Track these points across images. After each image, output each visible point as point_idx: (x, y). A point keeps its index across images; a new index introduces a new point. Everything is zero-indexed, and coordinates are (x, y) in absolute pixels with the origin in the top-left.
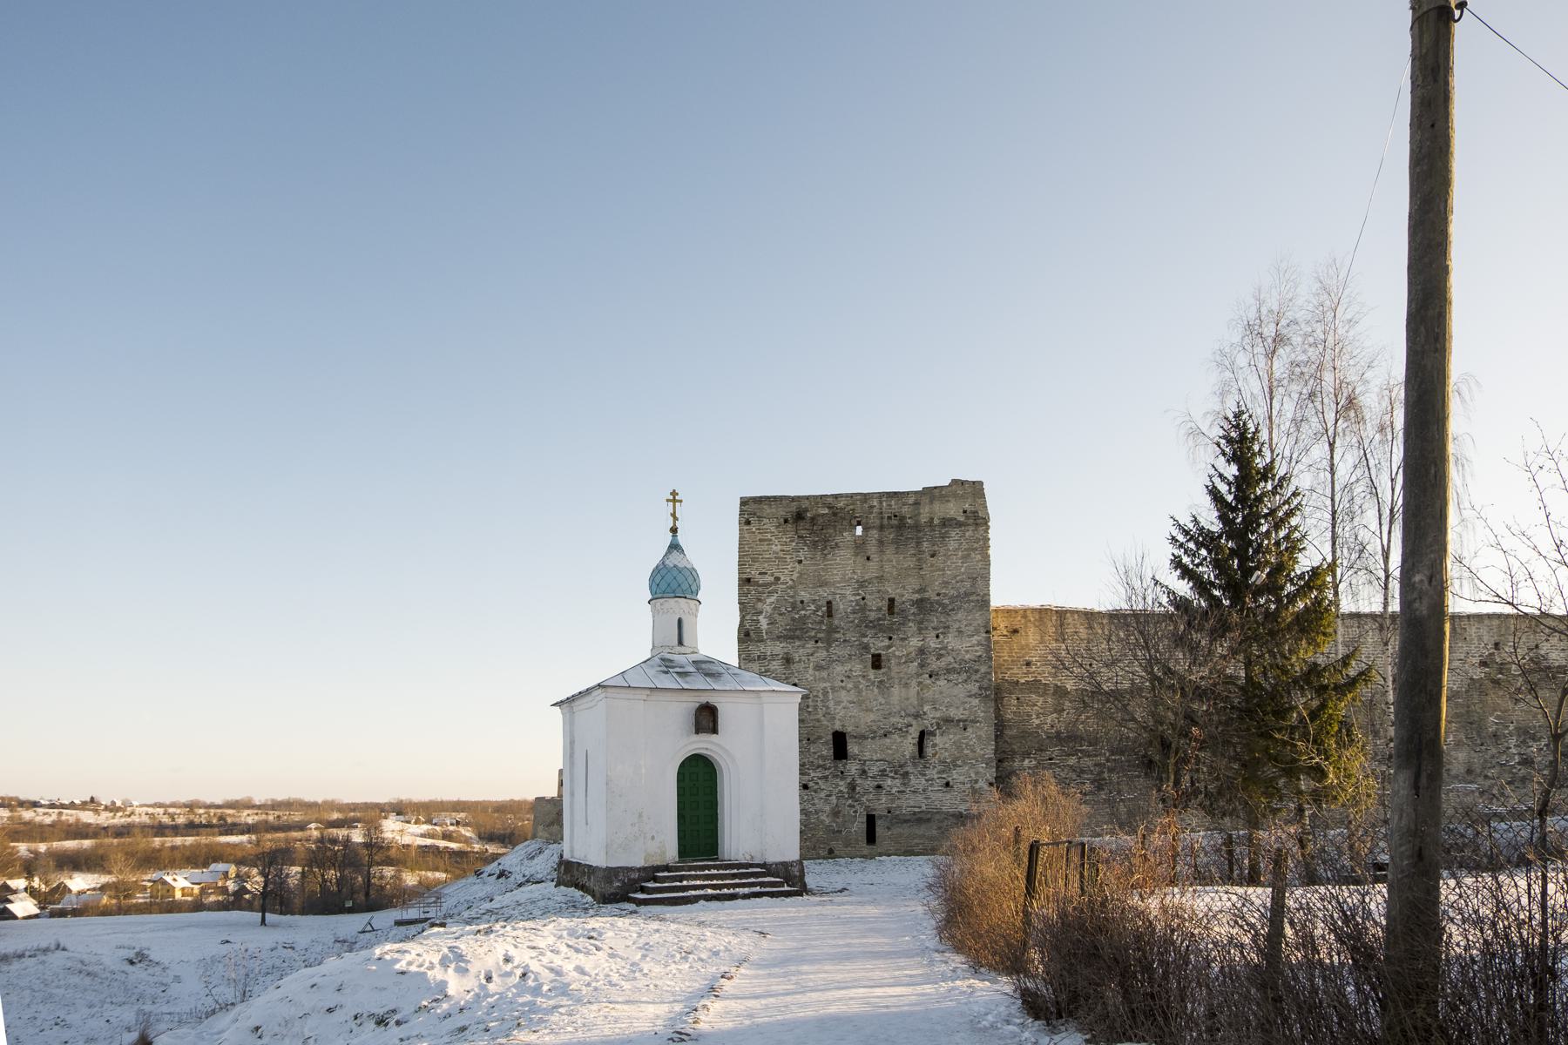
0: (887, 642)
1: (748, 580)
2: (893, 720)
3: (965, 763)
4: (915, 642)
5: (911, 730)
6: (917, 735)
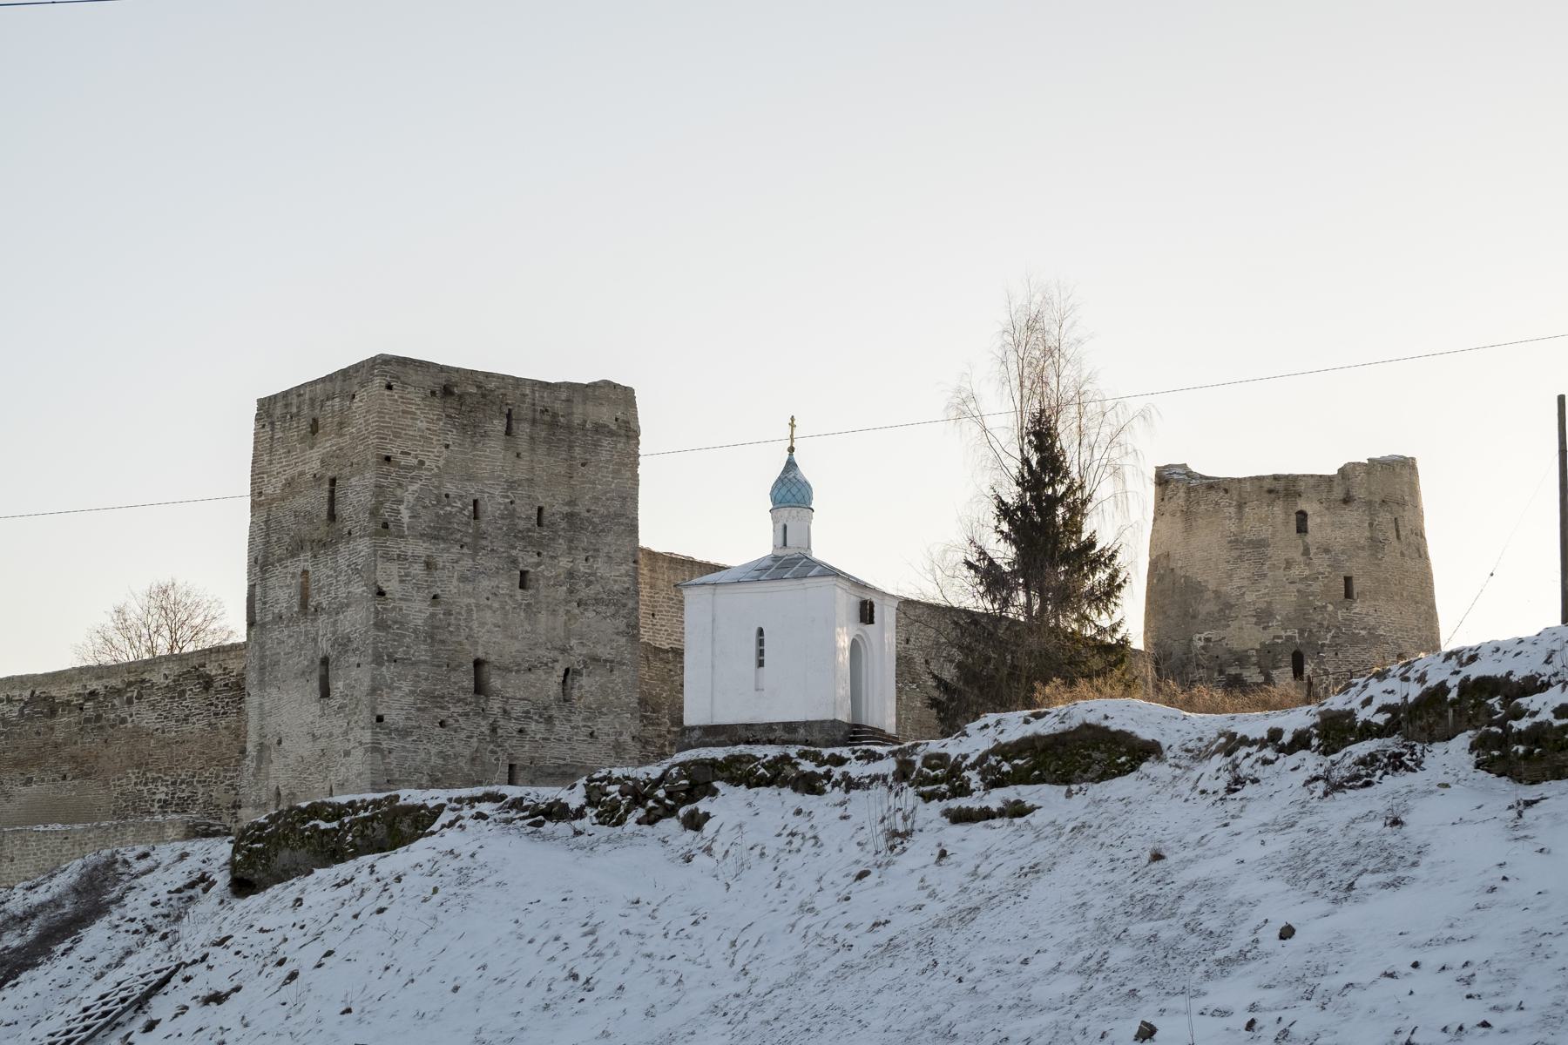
0: (536, 559)
1: (388, 459)
2: (539, 652)
3: (611, 712)
4: (564, 562)
5: (558, 666)
6: (562, 673)
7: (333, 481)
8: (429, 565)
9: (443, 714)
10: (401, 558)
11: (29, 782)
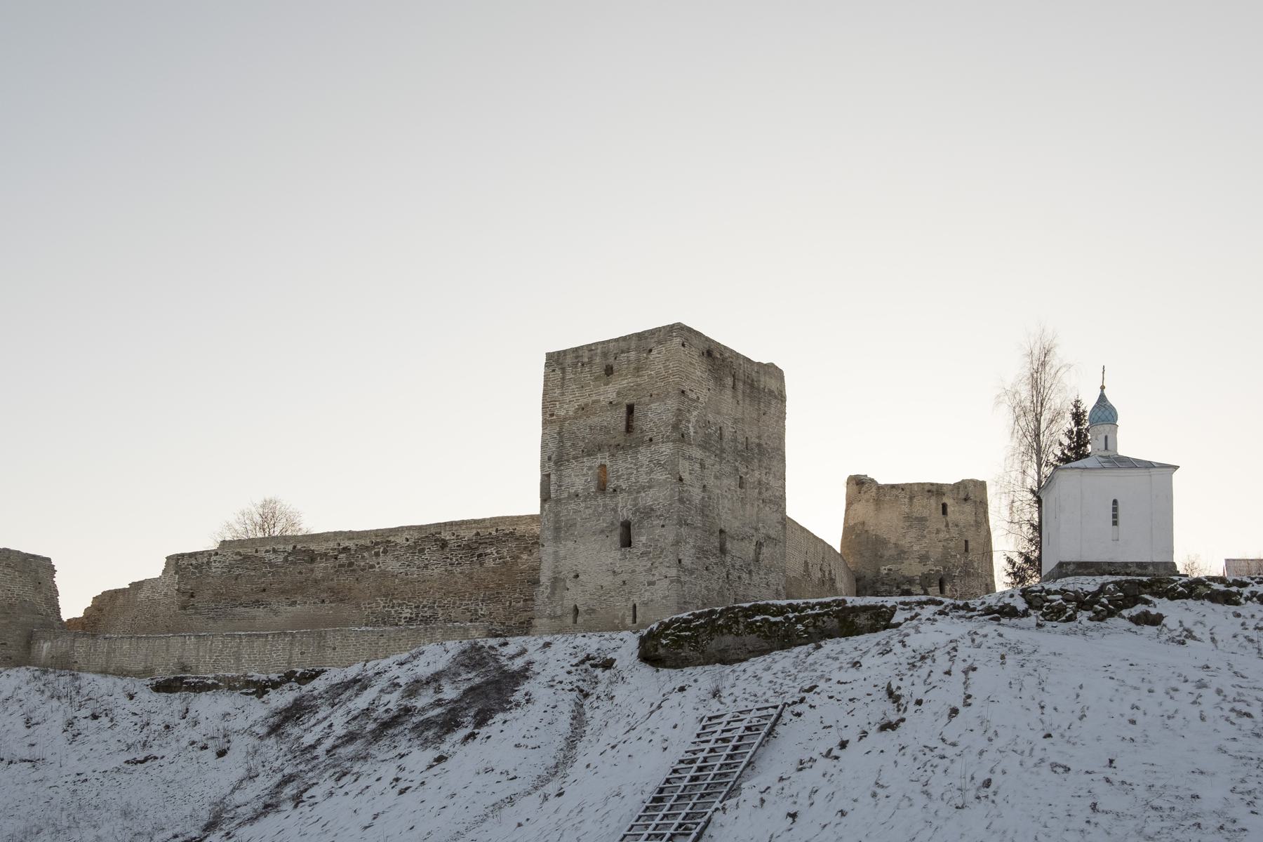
7: (630, 409)
8: (702, 466)
10: (690, 458)
11: (294, 603)
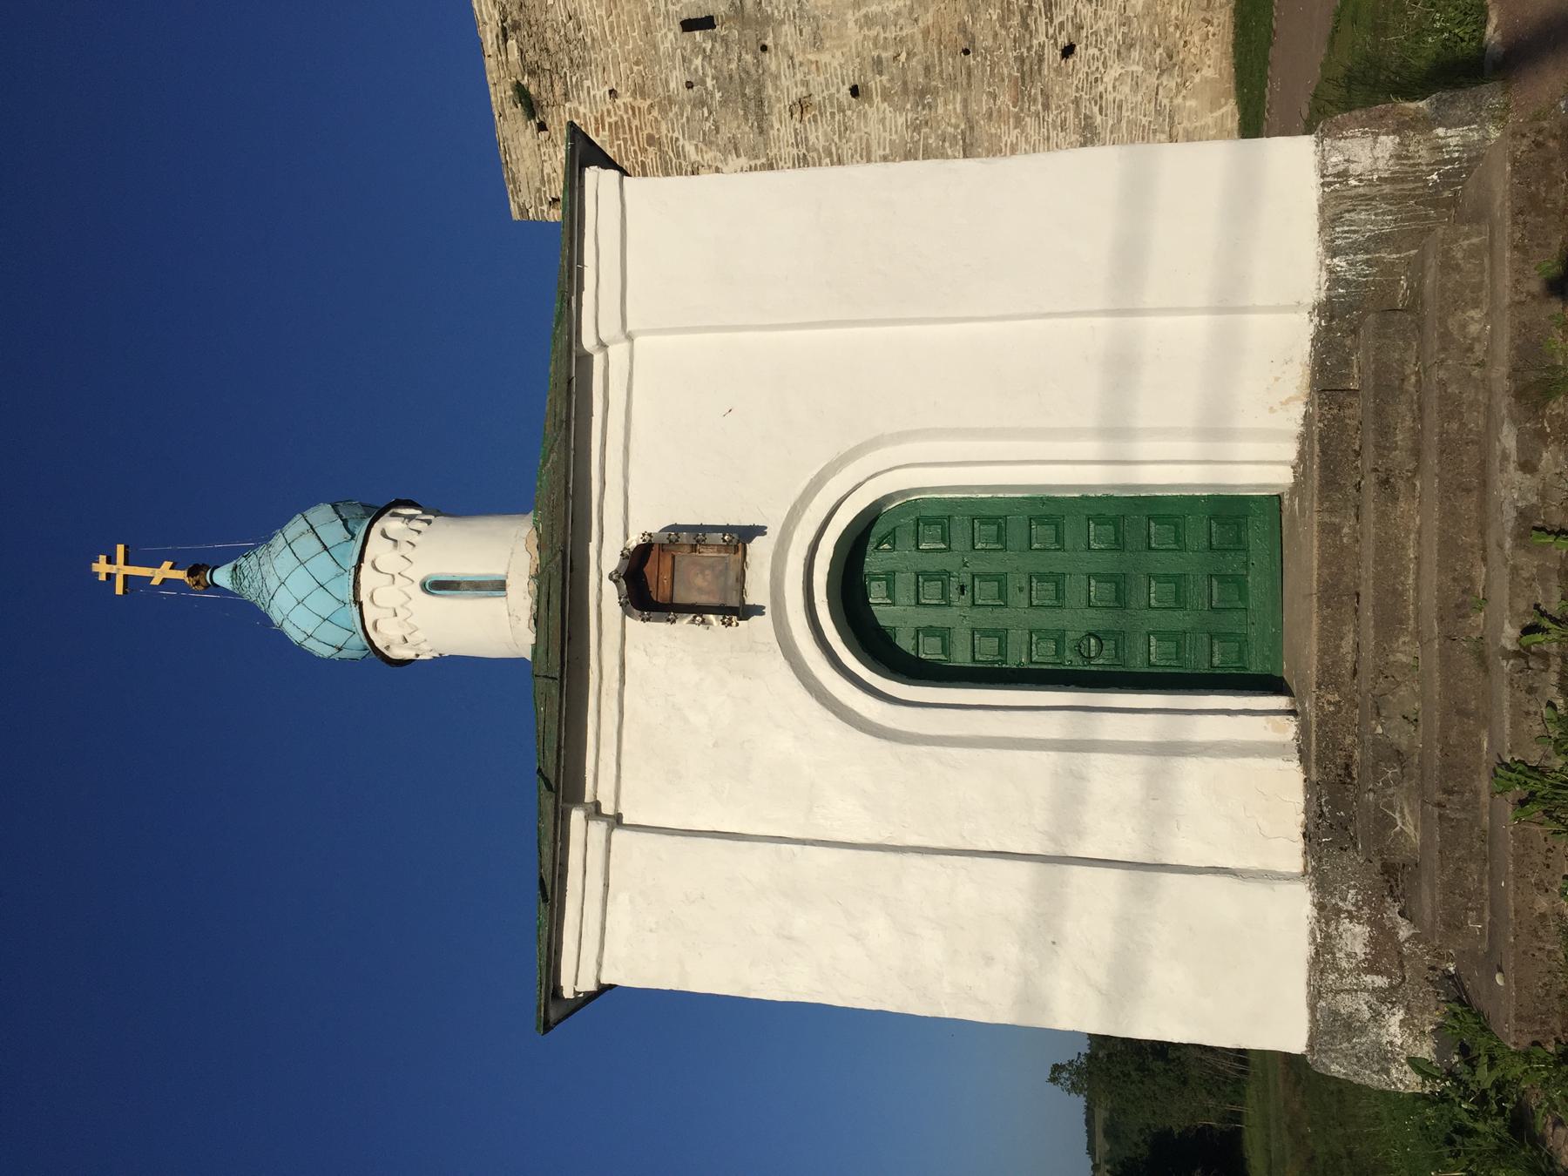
9: (1052, 55)
